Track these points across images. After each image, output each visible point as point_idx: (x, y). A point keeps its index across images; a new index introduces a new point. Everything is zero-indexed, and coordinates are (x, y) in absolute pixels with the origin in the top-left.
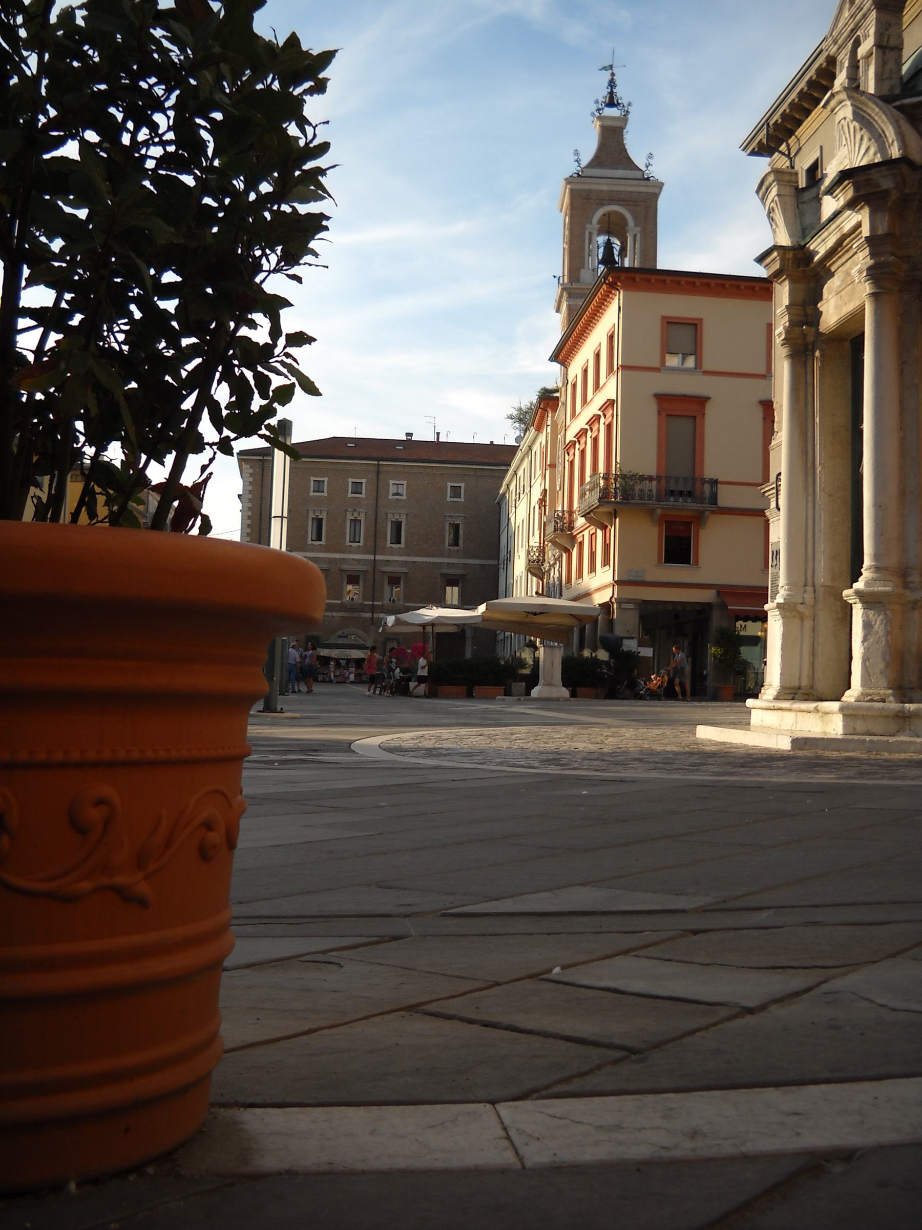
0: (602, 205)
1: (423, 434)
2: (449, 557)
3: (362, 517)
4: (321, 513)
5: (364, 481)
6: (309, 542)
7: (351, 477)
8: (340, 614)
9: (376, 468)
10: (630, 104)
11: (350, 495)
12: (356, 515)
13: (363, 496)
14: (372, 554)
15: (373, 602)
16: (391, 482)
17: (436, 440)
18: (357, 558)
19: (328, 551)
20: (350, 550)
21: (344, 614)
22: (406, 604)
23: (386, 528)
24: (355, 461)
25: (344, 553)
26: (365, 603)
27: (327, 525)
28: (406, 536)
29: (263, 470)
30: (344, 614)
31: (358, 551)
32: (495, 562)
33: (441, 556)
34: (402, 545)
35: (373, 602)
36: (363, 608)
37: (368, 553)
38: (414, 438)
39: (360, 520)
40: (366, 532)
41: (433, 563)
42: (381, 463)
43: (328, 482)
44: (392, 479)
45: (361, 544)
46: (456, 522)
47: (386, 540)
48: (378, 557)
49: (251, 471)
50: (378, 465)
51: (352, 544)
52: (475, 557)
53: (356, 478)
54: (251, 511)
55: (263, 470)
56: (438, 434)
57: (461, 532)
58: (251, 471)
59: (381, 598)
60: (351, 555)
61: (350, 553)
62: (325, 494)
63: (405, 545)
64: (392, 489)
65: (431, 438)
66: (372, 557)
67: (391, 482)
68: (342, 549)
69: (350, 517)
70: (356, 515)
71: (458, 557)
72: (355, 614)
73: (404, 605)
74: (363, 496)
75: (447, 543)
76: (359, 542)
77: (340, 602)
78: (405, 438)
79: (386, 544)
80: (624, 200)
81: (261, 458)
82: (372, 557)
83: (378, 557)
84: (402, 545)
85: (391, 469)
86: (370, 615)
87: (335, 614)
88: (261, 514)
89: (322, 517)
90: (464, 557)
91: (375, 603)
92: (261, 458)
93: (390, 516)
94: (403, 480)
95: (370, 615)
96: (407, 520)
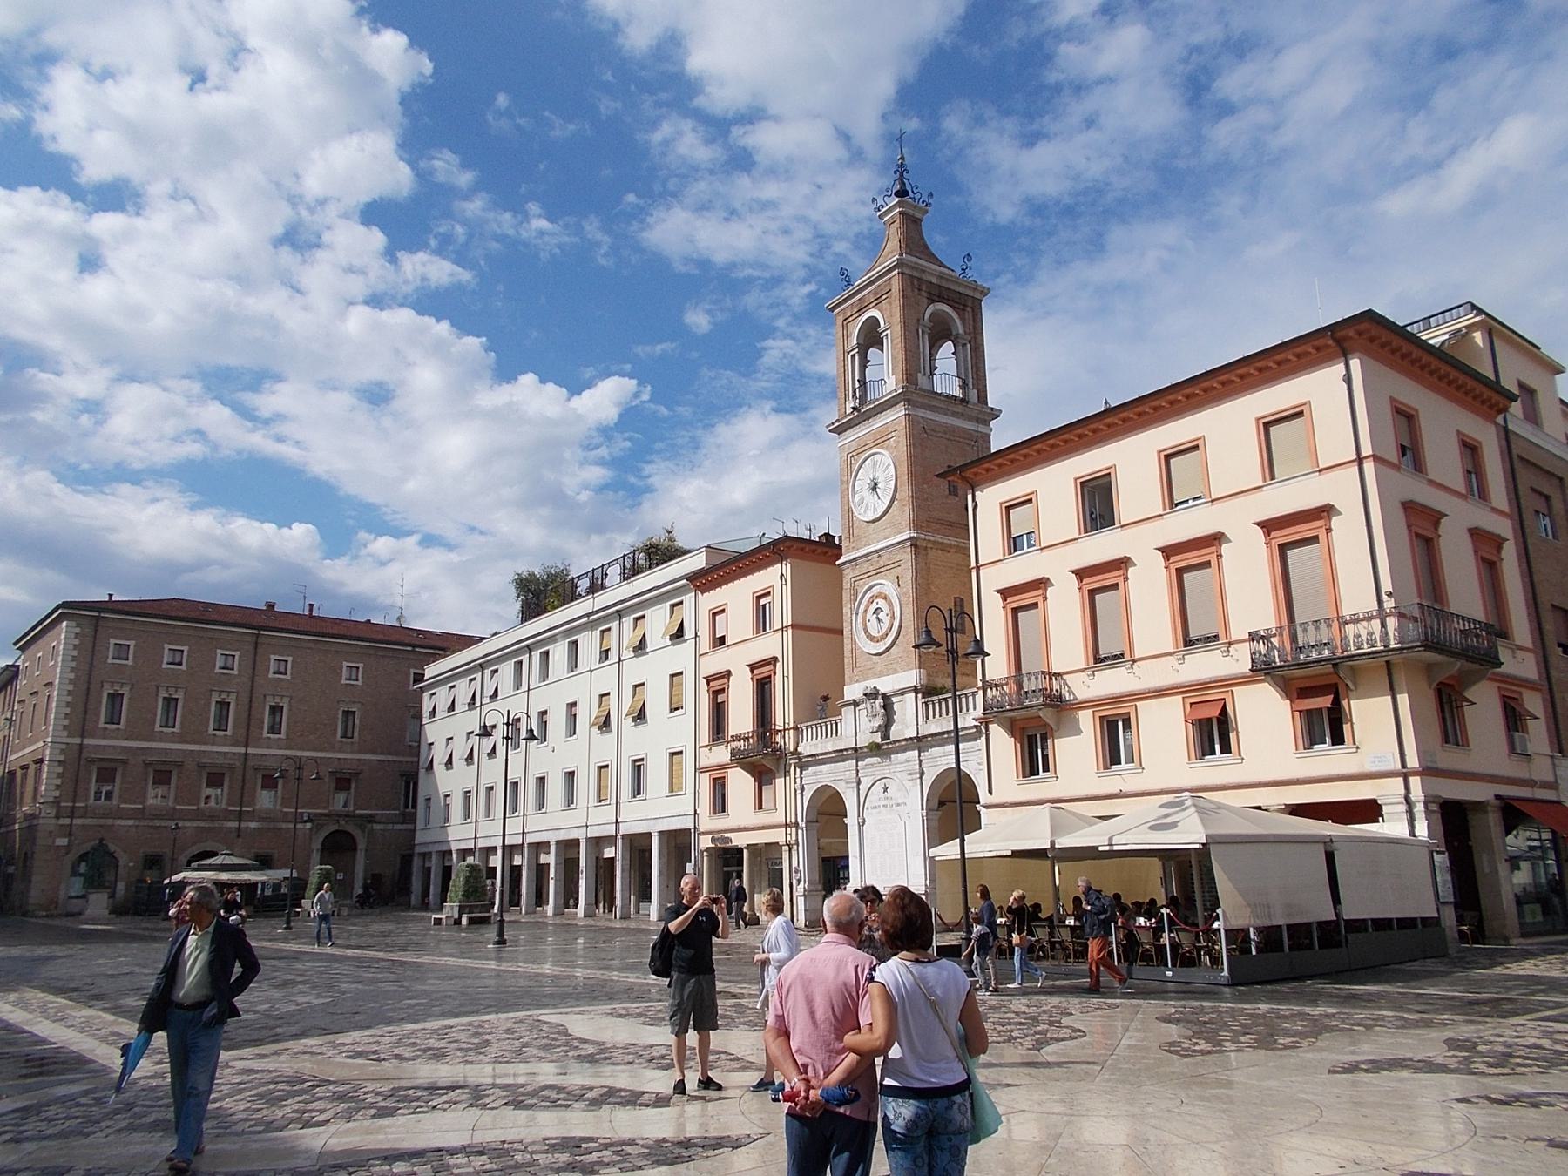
0: (932, 301)
2: (340, 751)
3: (232, 699)
6: (158, 728)
7: (221, 648)
8: (196, 824)
9: (255, 638)
10: (931, 195)
13: (235, 672)
16: (273, 657)
17: (307, 613)
18: (222, 749)
21: (202, 824)
22: (285, 810)
23: (263, 713)
24: (228, 629)
25: (205, 743)
26: (231, 808)
27: (183, 707)
28: (288, 725)
29: (96, 631)
30: (202, 824)
32: (416, 759)
33: (332, 749)
34: (283, 736)
36: (227, 815)
37: (235, 744)
39: (229, 703)
40: (235, 720)
43: (188, 652)
44: (275, 654)
47: (262, 728)
49: (78, 630)
50: (258, 636)
52: (374, 752)
54: (75, 684)
55: (96, 631)
56: (311, 605)
57: (357, 721)
58: (78, 630)
59: (252, 802)
61: (213, 744)
63: (287, 735)
65: (298, 608)
66: (243, 750)
68: (151, 737)
71: (352, 752)
72: (216, 824)
73: (175, 809)
74: (235, 672)
75: (339, 734)
77: (195, 808)
81: (96, 614)
82: (243, 750)
83: (250, 750)
84: (283, 736)
85: (274, 641)
86: (235, 824)
88: (88, 689)
90: (360, 752)
92: (96, 614)
93: (268, 698)
95: (235, 824)
96: (290, 705)
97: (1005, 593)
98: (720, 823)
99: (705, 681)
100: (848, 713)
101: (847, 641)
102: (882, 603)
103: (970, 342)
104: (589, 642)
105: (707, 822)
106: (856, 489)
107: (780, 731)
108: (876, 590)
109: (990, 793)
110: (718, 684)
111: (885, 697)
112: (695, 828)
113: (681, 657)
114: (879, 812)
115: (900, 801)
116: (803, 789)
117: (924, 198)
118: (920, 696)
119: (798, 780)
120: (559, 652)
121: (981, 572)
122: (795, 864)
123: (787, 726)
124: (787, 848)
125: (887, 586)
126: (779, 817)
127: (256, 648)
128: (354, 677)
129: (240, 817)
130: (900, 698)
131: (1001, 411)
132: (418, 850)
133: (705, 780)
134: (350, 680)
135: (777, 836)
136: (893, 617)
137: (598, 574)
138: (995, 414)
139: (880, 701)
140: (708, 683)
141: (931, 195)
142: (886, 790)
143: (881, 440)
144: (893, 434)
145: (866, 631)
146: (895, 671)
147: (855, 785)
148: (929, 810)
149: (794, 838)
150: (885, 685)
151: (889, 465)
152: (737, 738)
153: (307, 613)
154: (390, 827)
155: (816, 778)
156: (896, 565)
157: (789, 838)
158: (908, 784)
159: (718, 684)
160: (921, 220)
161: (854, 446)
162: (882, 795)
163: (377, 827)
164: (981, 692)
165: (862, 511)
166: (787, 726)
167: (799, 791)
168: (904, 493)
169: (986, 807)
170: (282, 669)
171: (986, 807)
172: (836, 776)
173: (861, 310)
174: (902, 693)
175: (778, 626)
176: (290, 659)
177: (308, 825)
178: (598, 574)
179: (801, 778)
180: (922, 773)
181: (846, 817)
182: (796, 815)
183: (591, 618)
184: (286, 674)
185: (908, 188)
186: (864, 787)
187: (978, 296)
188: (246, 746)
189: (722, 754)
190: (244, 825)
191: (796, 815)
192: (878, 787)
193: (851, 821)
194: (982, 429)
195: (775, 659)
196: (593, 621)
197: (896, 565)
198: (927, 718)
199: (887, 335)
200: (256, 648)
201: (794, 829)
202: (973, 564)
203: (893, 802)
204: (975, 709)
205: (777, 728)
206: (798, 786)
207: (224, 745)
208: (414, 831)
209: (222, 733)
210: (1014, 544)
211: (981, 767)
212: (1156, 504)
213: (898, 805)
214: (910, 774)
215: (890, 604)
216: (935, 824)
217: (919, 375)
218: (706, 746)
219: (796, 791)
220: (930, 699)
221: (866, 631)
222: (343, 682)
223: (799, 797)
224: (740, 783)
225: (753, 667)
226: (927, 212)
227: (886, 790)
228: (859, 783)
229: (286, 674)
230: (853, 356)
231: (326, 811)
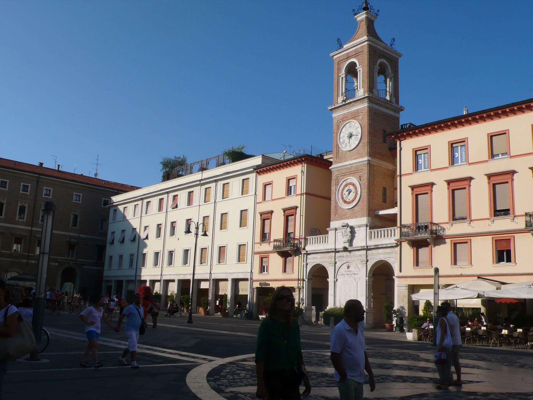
0: (380, 58)
1: (49, 164)
3: (26, 205)
4: (3, 200)
5: (30, 185)
10: (378, 11)
11: (21, 192)
12: (23, 203)
13: (28, 193)
14: (30, 227)
15: (29, 254)
16: (45, 188)
19: (5, 223)
20: (18, 223)
21: (12, 260)
26: (24, 254)
30: (12, 260)
31: (23, 224)
35: (29, 254)
37: (27, 225)
38: (44, 166)
39: (25, 207)
41: (61, 234)
42: (41, 176)
45: (25, 220)
46: (76, 214)
47: (39, 219)
48: (34, 229)
50: (39, 178)
51: (20, 220)
53: (25, 183)
56: (59, 166)
57: (78, 219)
60: (19, 226)
61: (18, 224)
62: (7, 189)
64: (44, 192)
66: (30, 228)
67: (45, 188)
69: (20, 204)
70: (23, 203)
74: (28, 193)
75: (71, 225)
76: (23, 219)
77: (9, 252)
78: (38, 165)
79: (39, 222)
80: (388, 58)
82: (30, 228)
83: (34, 229)
86: (25, 261)
87: (6, 259)
89: (3, 202)
91: (30, 254)
94: (51, 188)
97: (413, 188)
98: (264, 276)
99: (259, 215)
100: (331, 234)
101: (333, 202)
102: (351, 187)
103: (393, 77)
104: (198, 192)
105: (257, 276)
106: (341, 136)
107: (298, 239)
108: (349, 181)
109: (401, 271)
110: (266, 217)
111: (352, 228)
112: (251, 278)
113: (247, 203)
114: (345, 277)
115: (355, 273)
116: (307, 264)
117: (376, 12)
118: (368, 228)
119: (305, 261)
120: (183, 196)
121: (402, 178)
122: (301, 297)
123: (301, 237)
124: (298, 289)
125: (354, 180)
126: (295, 276)
127: (38, 183)
128: (78, 199)
129: (28, 258)
130: (358, 229)
131: (404, 108)
132: (105, 279)
133: (257, 258)
134: (76, 200)
135: (294, 284)
136: (357, 194)
137: (204, 163)
138: (402, 109)
139: (349, 230)
140: (261, 215)
141: (378, 11)
142: (348, 267)
143: (354, 116)
144: (361, 114)
145: (343, 198)
146: (356, 217)
147: (334, 264)
148: (369, 277)
149: (302, 285)
150: (352, 222)
151: (358, 127)
152: (275, 241)
153: (57, 169)
154: (91, 267)
155: (313, 261)
156: (359, 171)
157: (299, 285)
158: (360, 266)
159: (266, 217)
160: (374, 21)
161: (342, 117)
162: (346, 269)
163: (85, 267)
164: (399, 229)
165: (344, 146)
166: (301, 237)
167: (305, 266)
168: (366, 140)
169: (398, 277)
170: (48, 193)
171: (398, 277)
172: (326, 261)
173: (348, 58)
174: (360, 226)
175: (299, 192)
176: (52, 189)
177: (57, 264)
178: (204, 163)
179: (307, 260)
180: (367, 261)
181: (328, 278)
182: (303, 275)
183: (202, 182)
184: (50, 196)
185: (369, 6)
186: (338, 265)
187: (397, 57)
188: (32, 227)
189: (267, 247)
190: (30, 261)
191: (303, 275)
192: (345, 267)
193: (331, 280)
194: (397, 115)
195: (297, 207)
196: (201, 183)
197: (359, 171)
198: (371, 238)
199: (360, 70)
200: (38, 183)
201: (302, 282)
202: (398, 173)
203: (351, 273)
204: (395, 236)
205: (296, 237)
206: (305, 263)
207: (22, 225)
208: (103, 270)
209: (22, 220)
210: (416, 167)
211: (397, 260)
212: (485, 155)
213: (354, 274)
214: (362, 261)
215: (356, 188)
216: (371, 283)
217: (374, 89)
218: (258, 243)
219: (304, 265)
220: (373, 230)
221: (343, 198)
222: (74, 201)
223: (305, 268)
224: (276, 261)
225: (285, 210)
226: (376, 18)
227: (348, 267)
228: (336, 263)
229: (50, 196)
230: (342, 78)
231: (64, 258)
